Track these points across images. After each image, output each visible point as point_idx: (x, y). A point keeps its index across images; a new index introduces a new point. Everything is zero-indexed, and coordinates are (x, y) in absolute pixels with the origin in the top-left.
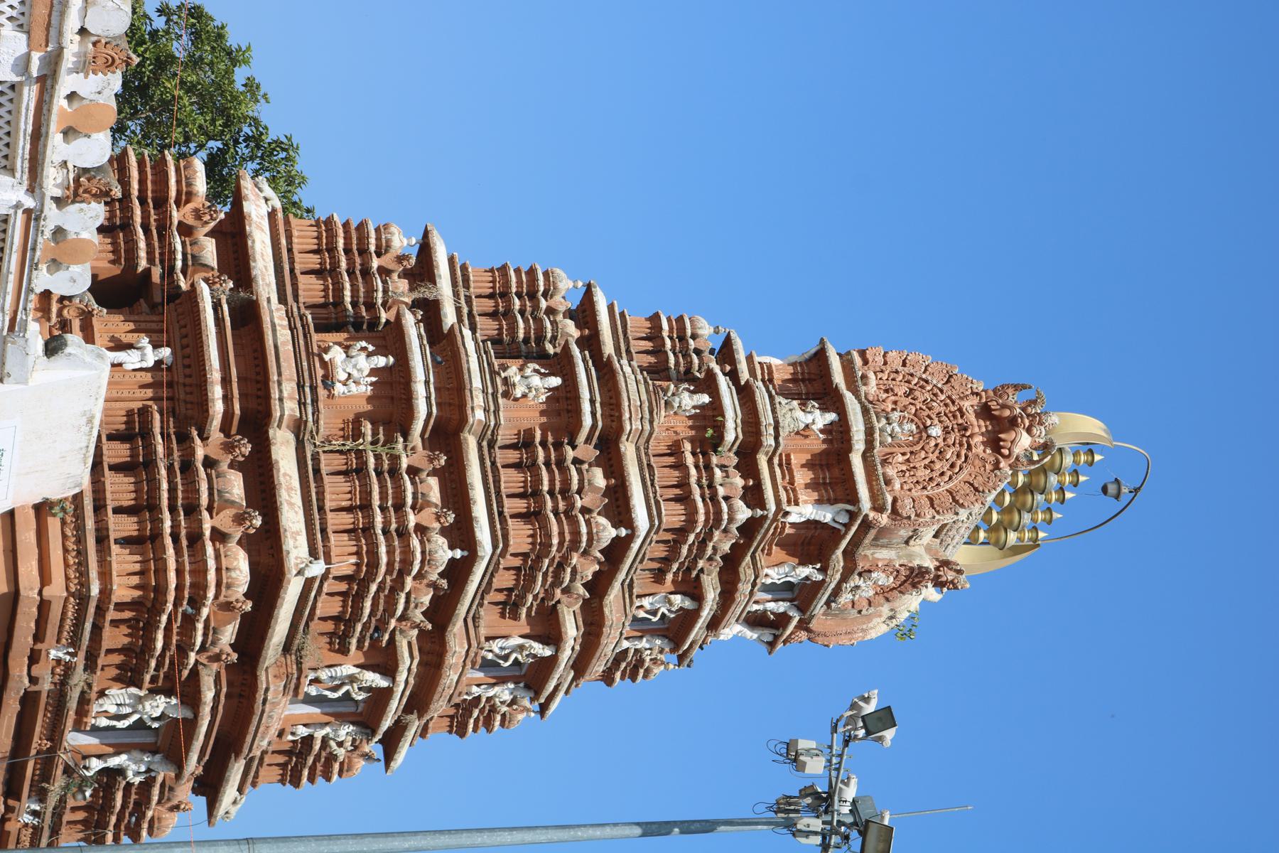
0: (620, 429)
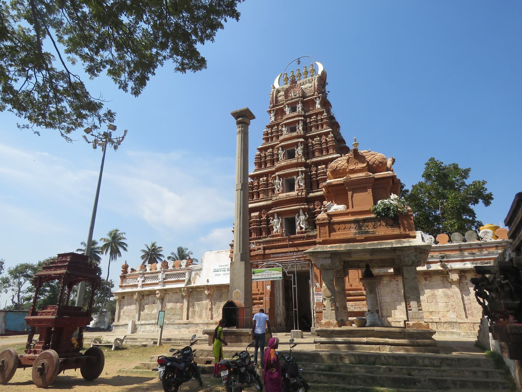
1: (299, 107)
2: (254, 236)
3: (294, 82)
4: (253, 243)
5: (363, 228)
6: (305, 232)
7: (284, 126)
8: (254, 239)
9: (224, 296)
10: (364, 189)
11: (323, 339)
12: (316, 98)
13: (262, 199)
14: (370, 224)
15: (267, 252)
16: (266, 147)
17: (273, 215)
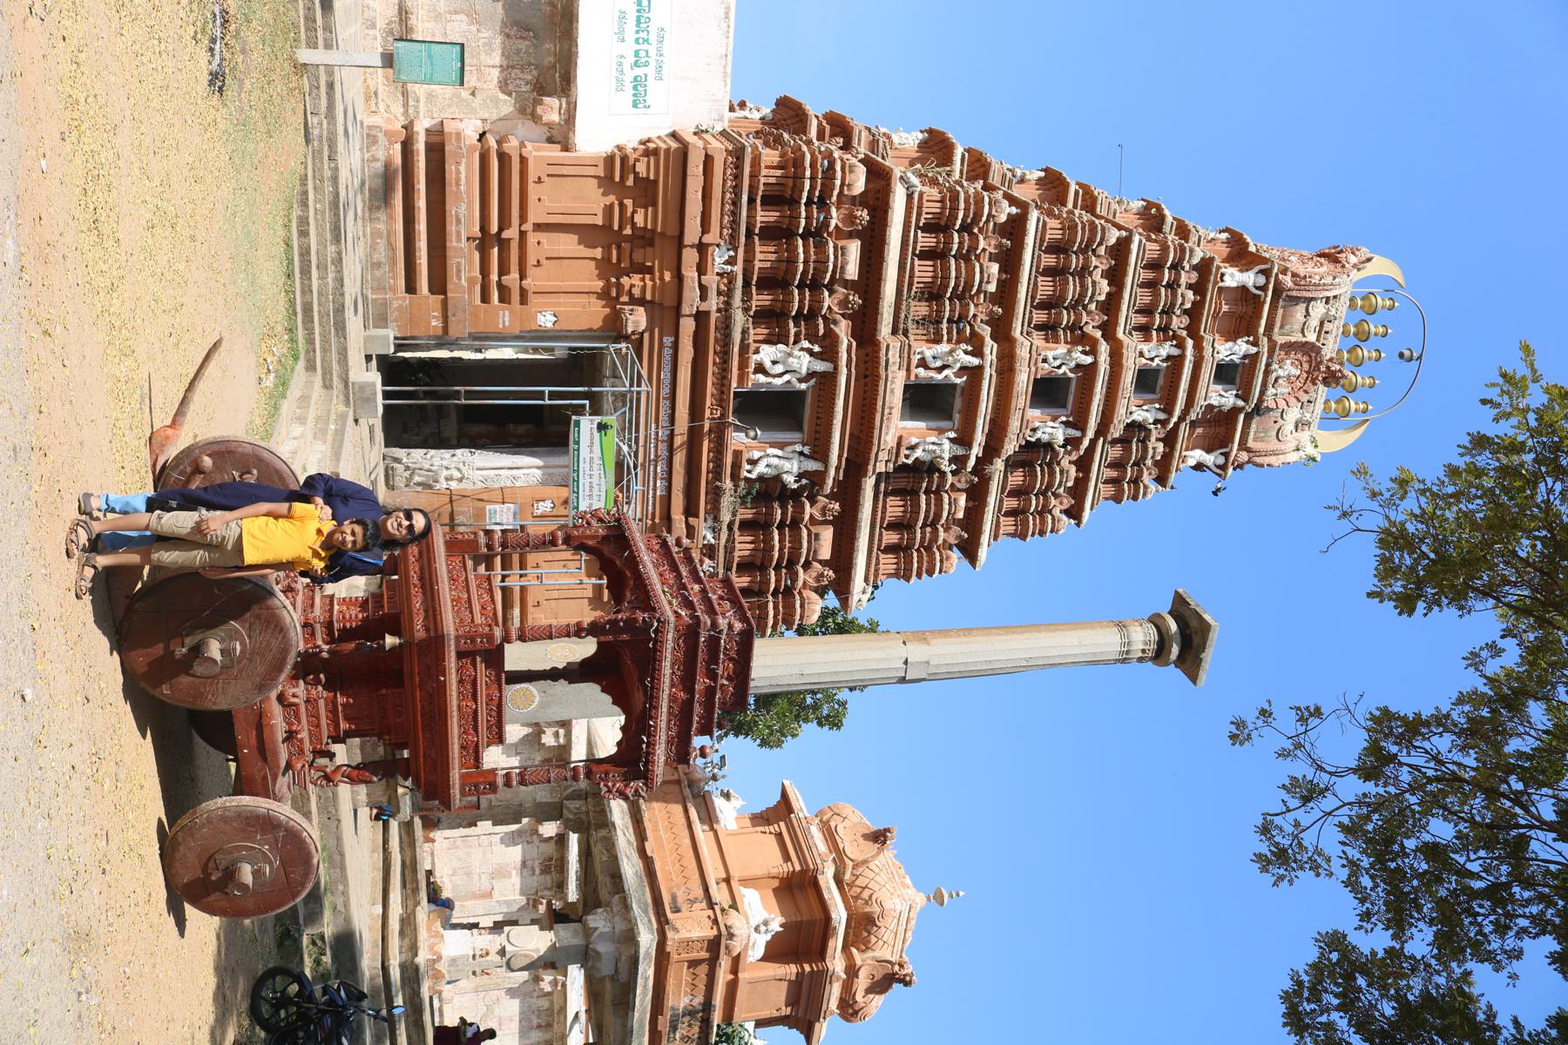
0: (1094, 199)
1: (1222, 397)
2: (764, 256)
3: (1331, 379)
4: (731, 261)
5: (687, 1019)
6: (735, 477)
7: (1175, 352)
8: (749, 261)
9: (523, 45)
10: (794, 998)
11: (395, 974)
12: (1226, 455)
13: (911, 277)
14: (696, 1029)
15: (688, 326)
16: (1124, 274)
17: (828, 351)
